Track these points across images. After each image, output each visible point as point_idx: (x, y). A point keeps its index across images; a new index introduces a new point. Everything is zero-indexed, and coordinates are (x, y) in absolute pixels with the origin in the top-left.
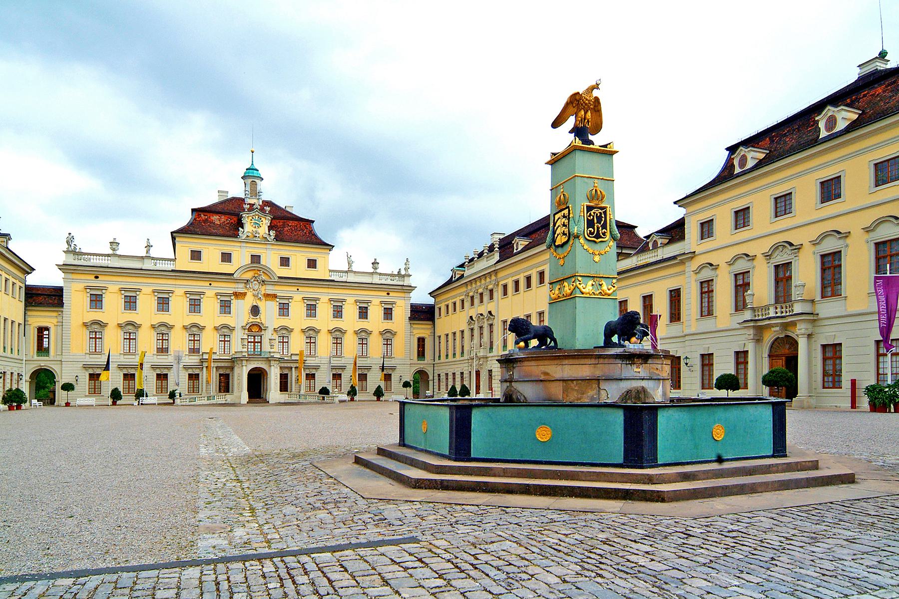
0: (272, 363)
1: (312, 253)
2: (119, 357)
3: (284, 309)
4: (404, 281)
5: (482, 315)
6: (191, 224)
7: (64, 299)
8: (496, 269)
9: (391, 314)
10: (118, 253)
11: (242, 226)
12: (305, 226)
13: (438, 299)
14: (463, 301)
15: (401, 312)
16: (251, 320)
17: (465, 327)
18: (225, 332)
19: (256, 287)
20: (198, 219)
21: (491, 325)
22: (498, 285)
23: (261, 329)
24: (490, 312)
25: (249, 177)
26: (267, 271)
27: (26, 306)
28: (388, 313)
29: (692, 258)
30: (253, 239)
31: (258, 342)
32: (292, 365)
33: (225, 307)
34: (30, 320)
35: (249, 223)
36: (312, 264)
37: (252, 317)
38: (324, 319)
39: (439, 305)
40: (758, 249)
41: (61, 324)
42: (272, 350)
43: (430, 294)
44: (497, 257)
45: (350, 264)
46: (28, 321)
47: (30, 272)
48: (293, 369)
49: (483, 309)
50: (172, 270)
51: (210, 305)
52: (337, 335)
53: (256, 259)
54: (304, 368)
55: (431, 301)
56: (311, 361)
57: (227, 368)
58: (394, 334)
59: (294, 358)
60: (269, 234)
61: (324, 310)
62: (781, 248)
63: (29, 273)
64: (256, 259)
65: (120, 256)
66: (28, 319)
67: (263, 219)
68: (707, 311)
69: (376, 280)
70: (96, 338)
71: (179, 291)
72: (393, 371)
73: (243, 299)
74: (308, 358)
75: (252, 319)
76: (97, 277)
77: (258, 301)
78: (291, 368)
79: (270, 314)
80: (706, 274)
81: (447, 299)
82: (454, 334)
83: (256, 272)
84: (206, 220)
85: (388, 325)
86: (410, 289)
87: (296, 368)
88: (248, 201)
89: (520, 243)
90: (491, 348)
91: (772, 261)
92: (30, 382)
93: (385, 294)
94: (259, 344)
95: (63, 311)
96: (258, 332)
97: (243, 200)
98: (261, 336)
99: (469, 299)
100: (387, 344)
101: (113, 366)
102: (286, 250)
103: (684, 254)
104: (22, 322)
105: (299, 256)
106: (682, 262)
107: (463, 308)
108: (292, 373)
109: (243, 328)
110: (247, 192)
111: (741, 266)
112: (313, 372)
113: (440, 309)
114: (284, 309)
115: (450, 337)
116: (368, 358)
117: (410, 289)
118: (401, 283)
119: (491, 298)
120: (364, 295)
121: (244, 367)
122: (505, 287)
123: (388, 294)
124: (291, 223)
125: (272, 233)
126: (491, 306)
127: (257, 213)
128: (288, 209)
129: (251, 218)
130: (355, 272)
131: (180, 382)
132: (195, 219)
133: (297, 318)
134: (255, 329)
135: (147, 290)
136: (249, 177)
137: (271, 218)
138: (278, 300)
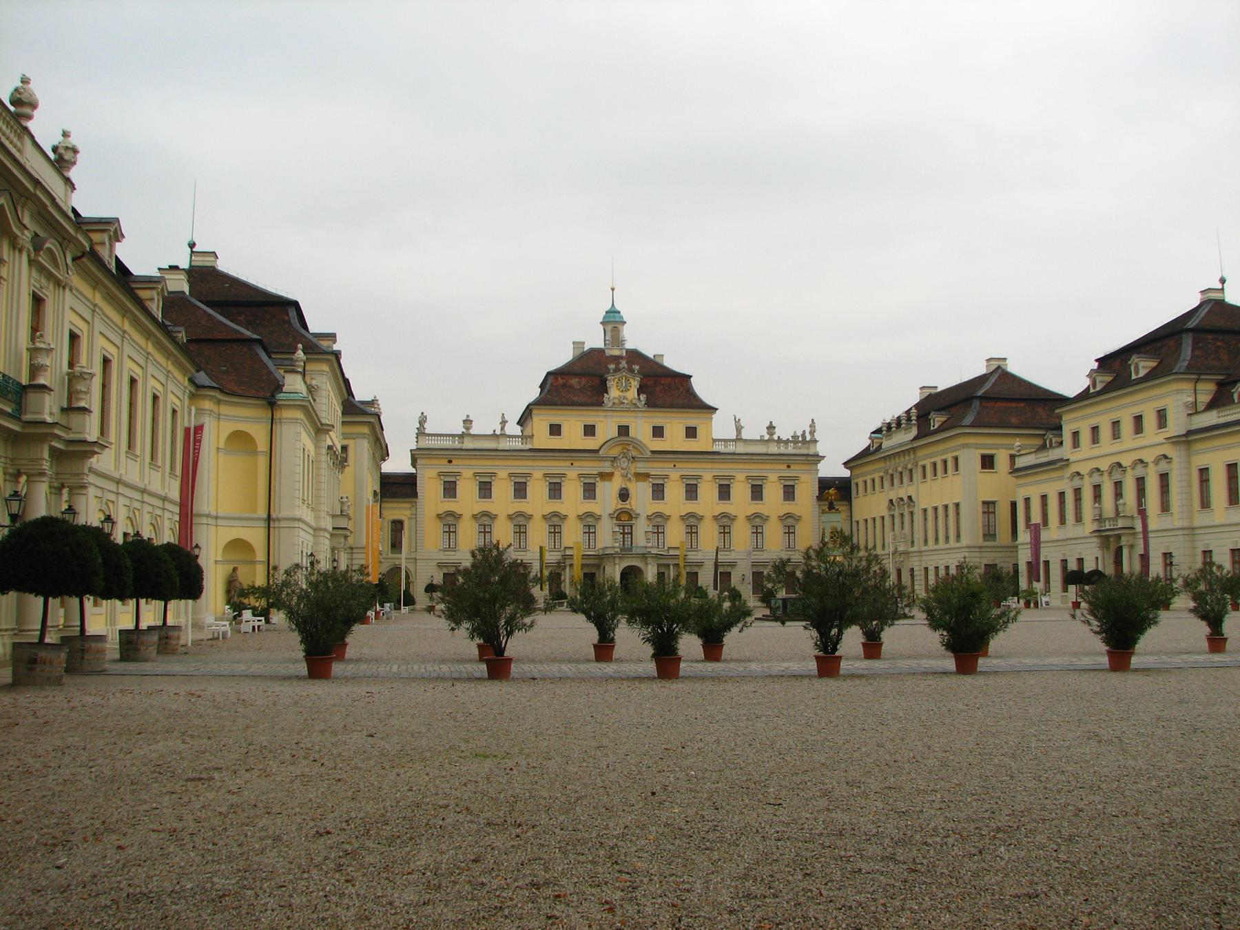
0: (649, 560)
1: (692, 419)
3: (658, 492)
4: (808, 449)
5: (902, 499)
8: (915, 445)
9: (794, 493)
10: (472, 432)
12: (681, 383)
13: (857, 472)
14: (882, 478)
15: (807, 491)
16: (620, 507)
17: (883, 510)
18: (589, 522)
19: (625, 465)
21: (912, 513)
22: (917, 466)
23: (631, 518)
24: (910, 498)
25: (610, 322)
26: (637, 445)
28: (789, 493)
29: (1068, 465)
30: (619, 406)
31: (628, 533)
32: (671, 562)
33: (590, 491)
34: (385, 513)
36: (691, 432)
39: (855, 481)
40: (1104, 465)
41: (414, 516)
42: (650, 545)
43: (844, 464)
44: (914, 432)
45: (739, 429)
48: (671, 567)
49: (903, 493)
50: (531, 450)
51: (572, 489)
52: (725, 523)
53: (624, 430)
55: (846, 473)
56: (693, 556)
57: (593, 565)
58: (798, 519)
59: (672, 552)
60: (639, 399)
61: (708, 491)
62: (1115, 469)
64: (624, 430)
65: (474, 436)
66: (383, 512)
67: (632, 381)
68: (1079, 518)
69: (774, 449)
70: (449, 532)
71: (538, 474)
73: (610, 480)
74: (688, 553)
75: (621, 505)
76: (450, 462)
77: (627, 483)
78: (668, 565)
80: (1077, 482)
81: (865, 474)
82: (874, 519)
83: (625, 446)
84: (564, 386)
85: (789, 507)
86: (818, 458)
87: (674, 565)
88: (608, 353)
89: (937, 420)
90: (913, 542)
91: (1113, 478)
93: (784, 467)
94: (629, 536)
97: (600, 352)
98: (631, 526)
99: (889, 477)
100: (789, 533)
102: (659, 418)
103: (1062, 460)
105: (675, 425)
106: (1062, 468)
107: (882, 488)
108: (669, 571)
110: (607, 342)
111: (1096, 479)
112: (695, 570)
113: (857, 485)
114: (658, 492)
115: (870, 523)
117: (818, 458)
118: (805, 451)
119: (911, 480)
120: (757, 470)
121: (617, 566)
122: (924, 467)
123: (789, 466)
125: (643, 397)
126: (911, 491)
128: (658, 360)
129: (616, 380)
130: (746, 441)
134: (625, 519)
135: (502, 474)
136: (610, 322)
138: (651, 480)
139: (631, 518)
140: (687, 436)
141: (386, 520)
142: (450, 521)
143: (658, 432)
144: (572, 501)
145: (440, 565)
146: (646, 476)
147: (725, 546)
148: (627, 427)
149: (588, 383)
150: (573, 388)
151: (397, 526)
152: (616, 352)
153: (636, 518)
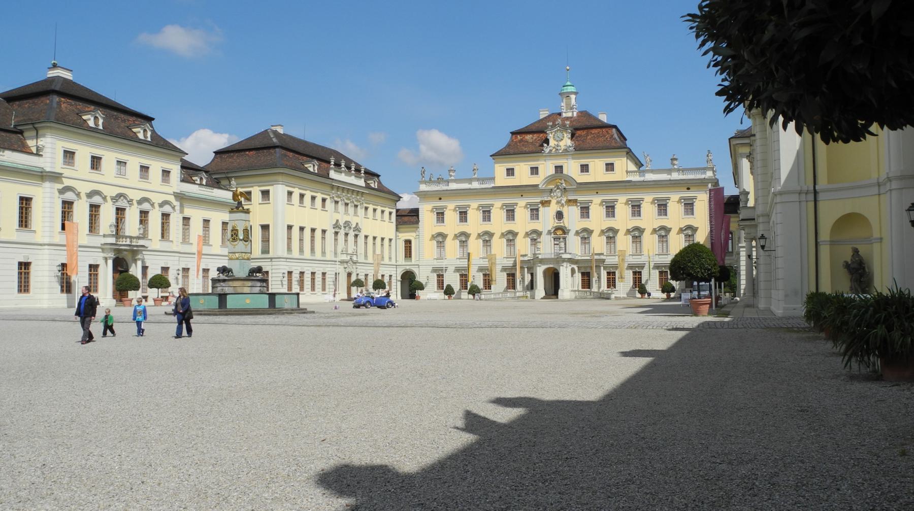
2: (502, 260)
3: (585, 211)
6: (509, 145)
7: (420, 218)
11: (547, 141)
12: (607, 132)
16: (556, 225)
18: (534, 236)
20: (515, 140)
26: (569, 179)
27: (397, 226)
30: (556, 154)
33: (534, 213)
35: (552, 138)
37: (557, 221)
38: (623, 219)
41: (418, 237)
46: (398, 236)
47: (398, 200)
51: (522, 213)
53: (559, 169)
54: (604, 267)
63: (397, 201)
64: (559, 169)
72: (617, 269)
74: (608, 257)
76: (440, 199)
79: (573, 219)
84: (521, 141)
88: (564, 115)
92: (401, 281)
95: (419, 228)
96: (562, 234)
97: (560, 114)
98: (565, 238)
101: (499, 267)
104: (393, 237)
109: (549, 233)
114: (585, 211)
116: (669, 256)
124: (594, 131)
127: (559, 128)
129: (553, 133)
131: (497, 279)
132: (512, 141)
133: (597, 219)
134: (560, 233)
137: (571, 130)
138: (579, 204)
139: (564, 233)
140: (607, 170)
141: (401, 240)
142: (440, 239)
143: (585, 168)
144: (522, 222)
145: (434, 270)
146: (574, 202)
147: (638, 252)
148: (561, 167)
149: (538, 137)
150: (527, 142)
151: (408, 243)
152: (570, 115)
153: (568, 232)
